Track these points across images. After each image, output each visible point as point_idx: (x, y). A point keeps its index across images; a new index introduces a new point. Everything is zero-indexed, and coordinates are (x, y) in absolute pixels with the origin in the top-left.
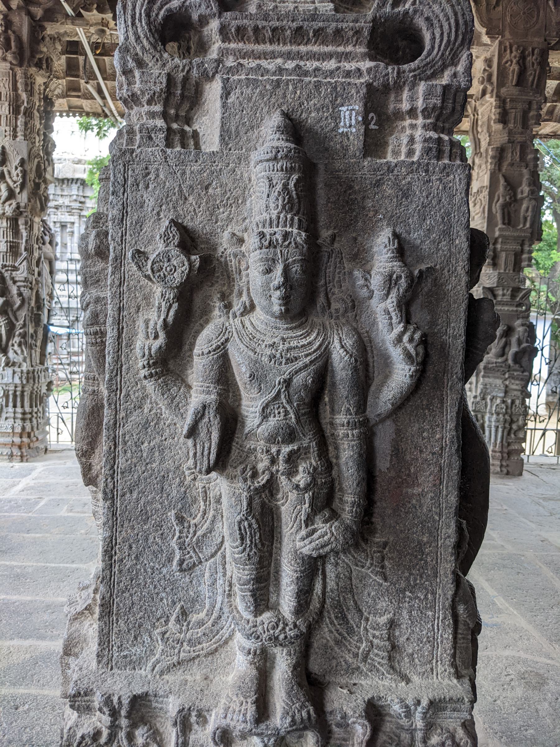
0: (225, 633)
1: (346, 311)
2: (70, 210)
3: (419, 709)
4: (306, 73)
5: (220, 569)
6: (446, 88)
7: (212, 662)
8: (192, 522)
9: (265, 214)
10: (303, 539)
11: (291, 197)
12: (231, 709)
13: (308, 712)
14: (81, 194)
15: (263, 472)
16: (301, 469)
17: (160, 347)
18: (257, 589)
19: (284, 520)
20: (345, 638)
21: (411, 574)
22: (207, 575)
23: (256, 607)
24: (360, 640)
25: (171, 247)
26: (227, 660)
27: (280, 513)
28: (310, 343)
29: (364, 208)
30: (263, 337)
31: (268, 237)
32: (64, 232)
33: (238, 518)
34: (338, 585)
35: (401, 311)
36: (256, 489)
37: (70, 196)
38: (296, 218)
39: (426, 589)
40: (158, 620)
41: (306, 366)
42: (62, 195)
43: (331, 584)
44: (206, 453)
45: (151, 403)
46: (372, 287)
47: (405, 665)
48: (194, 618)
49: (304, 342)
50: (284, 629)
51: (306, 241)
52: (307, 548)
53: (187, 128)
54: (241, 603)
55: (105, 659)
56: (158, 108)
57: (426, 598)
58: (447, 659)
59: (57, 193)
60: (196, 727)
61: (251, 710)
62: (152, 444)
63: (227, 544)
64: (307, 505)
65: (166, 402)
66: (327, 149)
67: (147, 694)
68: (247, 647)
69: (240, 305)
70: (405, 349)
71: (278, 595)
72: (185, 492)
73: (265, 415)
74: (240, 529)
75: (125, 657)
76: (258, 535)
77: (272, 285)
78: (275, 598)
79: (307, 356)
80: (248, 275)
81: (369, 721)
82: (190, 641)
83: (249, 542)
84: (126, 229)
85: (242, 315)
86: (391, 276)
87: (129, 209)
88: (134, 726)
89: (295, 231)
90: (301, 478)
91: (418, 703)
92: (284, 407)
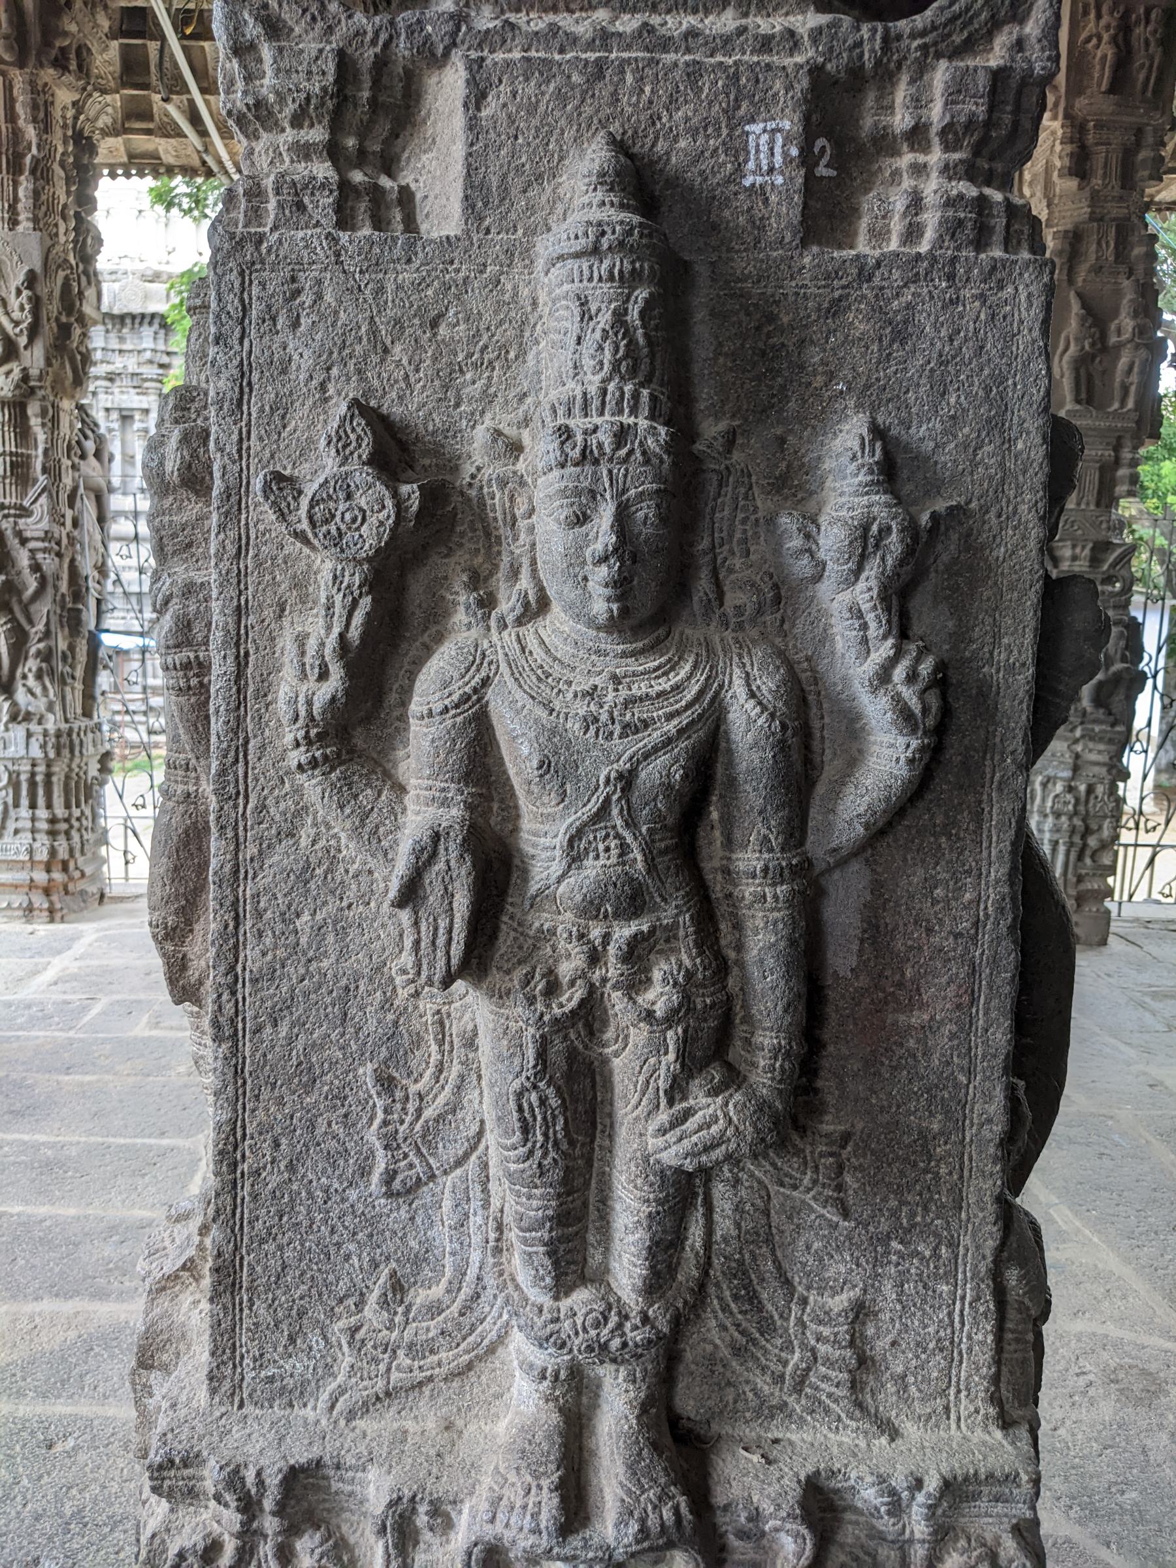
0: (489, 1330)
1: (760, 611)
2: (139, 383)
3: (920, 1498)
4: (666, 44)
5: (476, 1192)
6: (998, 76)
7: (461, 1393)
8: (413, 1089)
9: (571, 384)
10: (662, 1131)
11: (632, 343)
12: (504, 1502)
13: (676, 1510)
14: (161, 347)
15: (572, 983)
16: (657, 975)
17: (333, 699)
18: (560, 1239)
19: (618, 1089)
20: (754, 1342)
21: (902, 1203)
22: (447, 1204)
23: (557, 1278)
24: (788, 1347)
25: (354, 465)
26: (494, 1389)
27: (611, 1073)
28: (677, 688)
29: (802, 367)
30: (568, 675)
31: (579, 438)
32: (129, 430)
33: (516, 1085)
34: (738, 1226)
35: (888, 610)
36: (556, 1021)
37: (139, 352)
38: (645, 392)
39: (936, 1235)
40: (341, 1301)
41: (668, 742)
42: (120, 351)
43: (724, 1225)
44: (441, 941)
45: (315, 825)
46: (821, 555)
47: (887, 1400)
48: (420, 1297)
49: (664, 684)
50: (620, 1326)
51: (668, 448)
52: (673, 1150)
53: (385, 182)
54: (525, 1268)
55: (227, 1385)
56: (317, 134)
57: (936, 1254)
58: (981, 1386)
59: (110, 347)
60: (427, 1536)
61: (549, 1505)
62: (318, 917)
63: (491, 1138)
64: (671, 1056)
65: (348, 824)
66: (715, 227)
67: (319, 1463)
68: (539, 1363)
69: (514, 598)
70: (897, 698)
71: (607, 1251)
72: (396, 1023)
73: (575, 854)
74: (520, 1109)
75: (271, 1380)
76: (561, 1121)
77: (588, 553)
78: (599, 1257)
79: (670, 717)
80: (531, 530)
81: (811, 1527)
82: (411, 1346)
83: (540, 1138)
84: (249, 424)
85: (519, 622)
86: (866, 528)
87: (255, 376)
88: (292, 1530)
89: (643, 423)
90: (659, 995)
91: (919, 1484)
92: (617, 836)
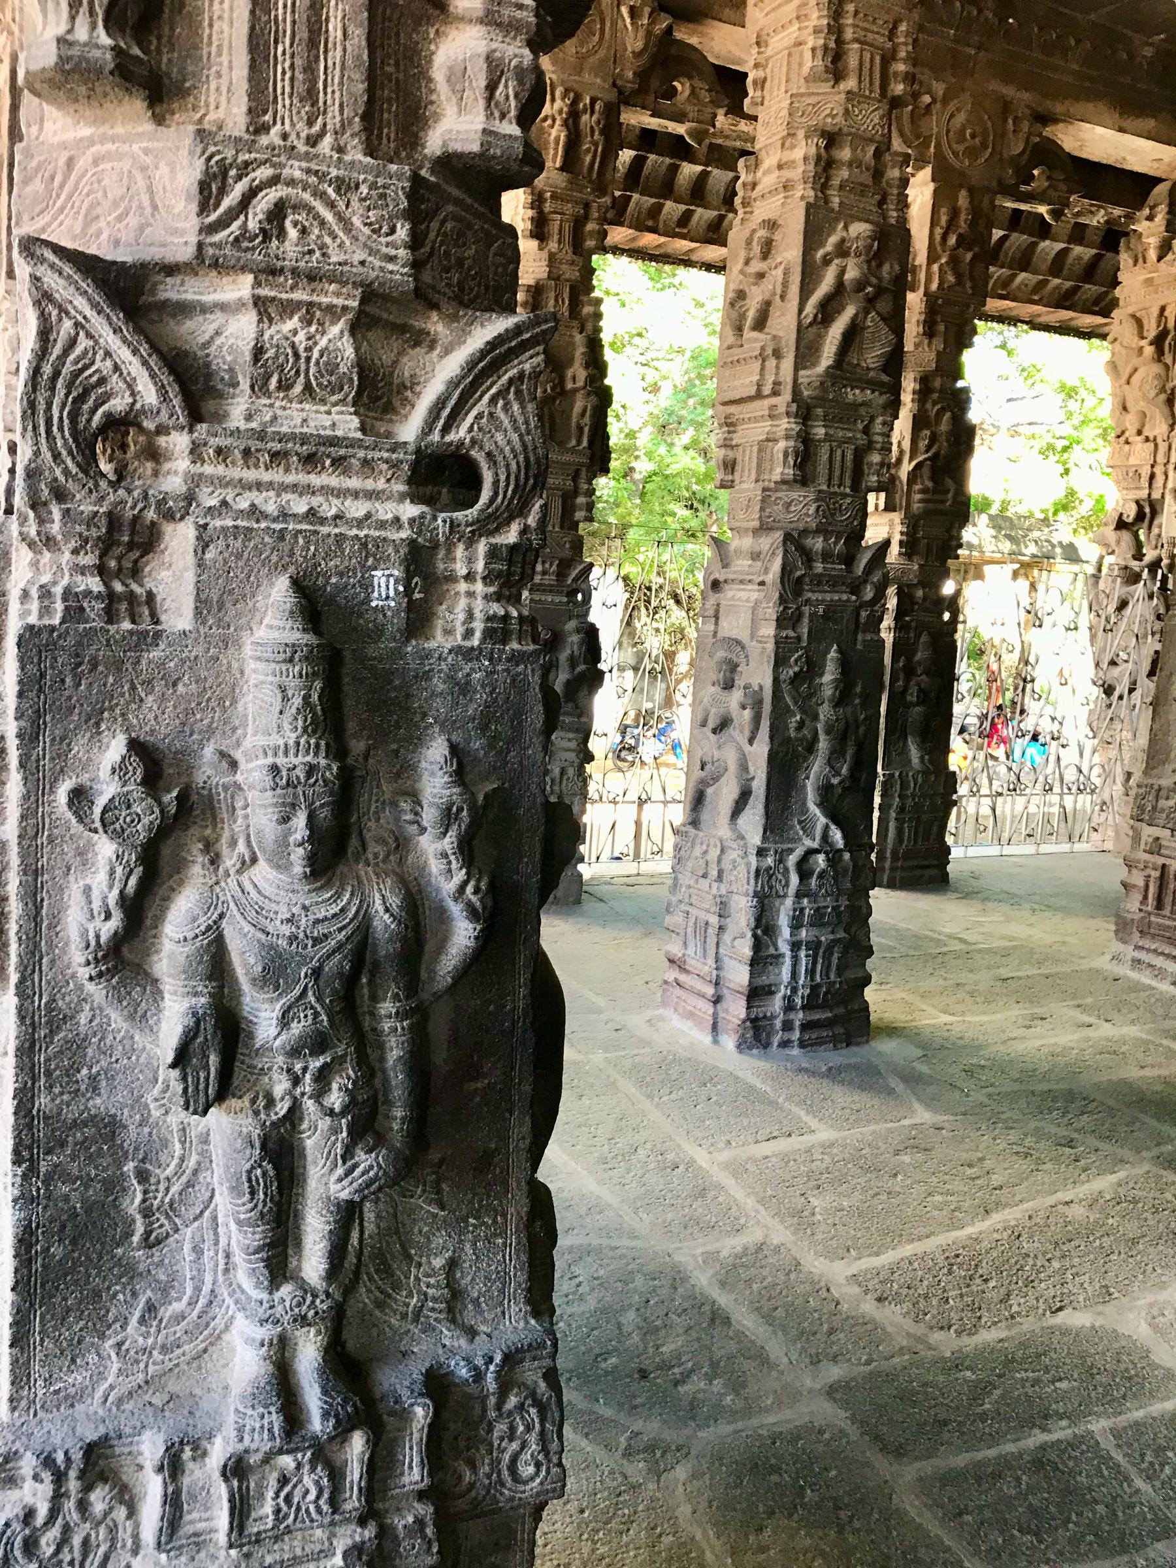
0: (219, 1323)
1: (387, 856)
3: (492, 1368)
4: (323, 521)
5: (209, 1236)
6: (513, 548)
7: (200, 1368)
8: (162, 1177)
9: (275, 736)
10: (340, 1180)
11: (315, 714)
12: (248, 1428)
13: (354, 1405)
15: (282, 1099)
16: (335, 1086)
17: (116, 933)
18: (273, 1256)
19: (309, 1159)
20: (389, 1296)
21: (475, 1195)
22: (187, 1247)
23: (271, 1282)
24: (410, 1295)
25: (131, 787)
26: (221, 1362)
27: (304, 1149)
28: (342, 910)
29: (408, 709)
30: (274, 907)
31: (284, 773)
33: (248, 1166)
34: (379, 1227)
35: (462, 853)
36: (273, 1123)
38: (323, 743)
39: (496, 1211)
40: (109, 1327)
41: (340, 946)
43: (370, 1227)
44: (202, 1086)
45: (92, 1009)
46: (425, 823)
47: (469, 1316)
48: (167, 1312)
49: (335, 909)
50: (313, 1302)
51: (338, 777)
52: (347, 1191)
53: (135, 587)
55: (24, 1403)
56: (89, 559)
57: (495, 1222)
58: (521, 1295)
60: (190, 1465)
61: (276, 1420)
62: (94, 1070)
63: (218, 1198)
64: (345, 1134)
65: (125, 1012)
66: (355, 629)
67: (106, 1438)
68: (259, 1337)
69: (235, 859)
71: (299, 1261)
72: (150, 1134)
73: (284, 1021)
74: (250, 1180)
75: (57, 1392)
76: (276, 1184)
77: (291, 840)
78: (295, 1263)
79: (340, 930)
80: (246, 817)
81: (431, 1399)
82: (163, 1347)
83: (262, 1196)
84: (44, 749)
85: (239, 872)
86: (449, 809)
87: (48, 718)
88: (88, 1488)
89: (323, 762)
90: (335, 1099)
91: (490, 1360)
92: (312, 1008)
